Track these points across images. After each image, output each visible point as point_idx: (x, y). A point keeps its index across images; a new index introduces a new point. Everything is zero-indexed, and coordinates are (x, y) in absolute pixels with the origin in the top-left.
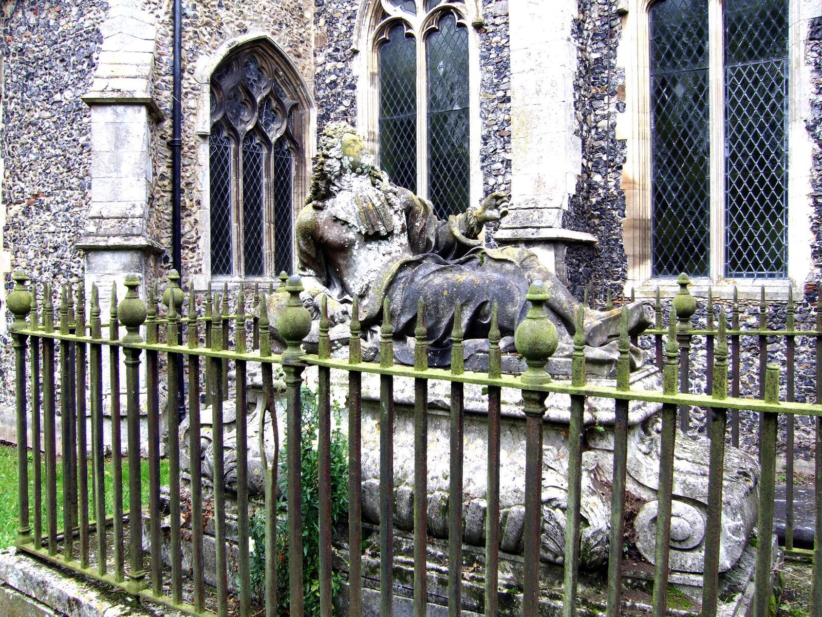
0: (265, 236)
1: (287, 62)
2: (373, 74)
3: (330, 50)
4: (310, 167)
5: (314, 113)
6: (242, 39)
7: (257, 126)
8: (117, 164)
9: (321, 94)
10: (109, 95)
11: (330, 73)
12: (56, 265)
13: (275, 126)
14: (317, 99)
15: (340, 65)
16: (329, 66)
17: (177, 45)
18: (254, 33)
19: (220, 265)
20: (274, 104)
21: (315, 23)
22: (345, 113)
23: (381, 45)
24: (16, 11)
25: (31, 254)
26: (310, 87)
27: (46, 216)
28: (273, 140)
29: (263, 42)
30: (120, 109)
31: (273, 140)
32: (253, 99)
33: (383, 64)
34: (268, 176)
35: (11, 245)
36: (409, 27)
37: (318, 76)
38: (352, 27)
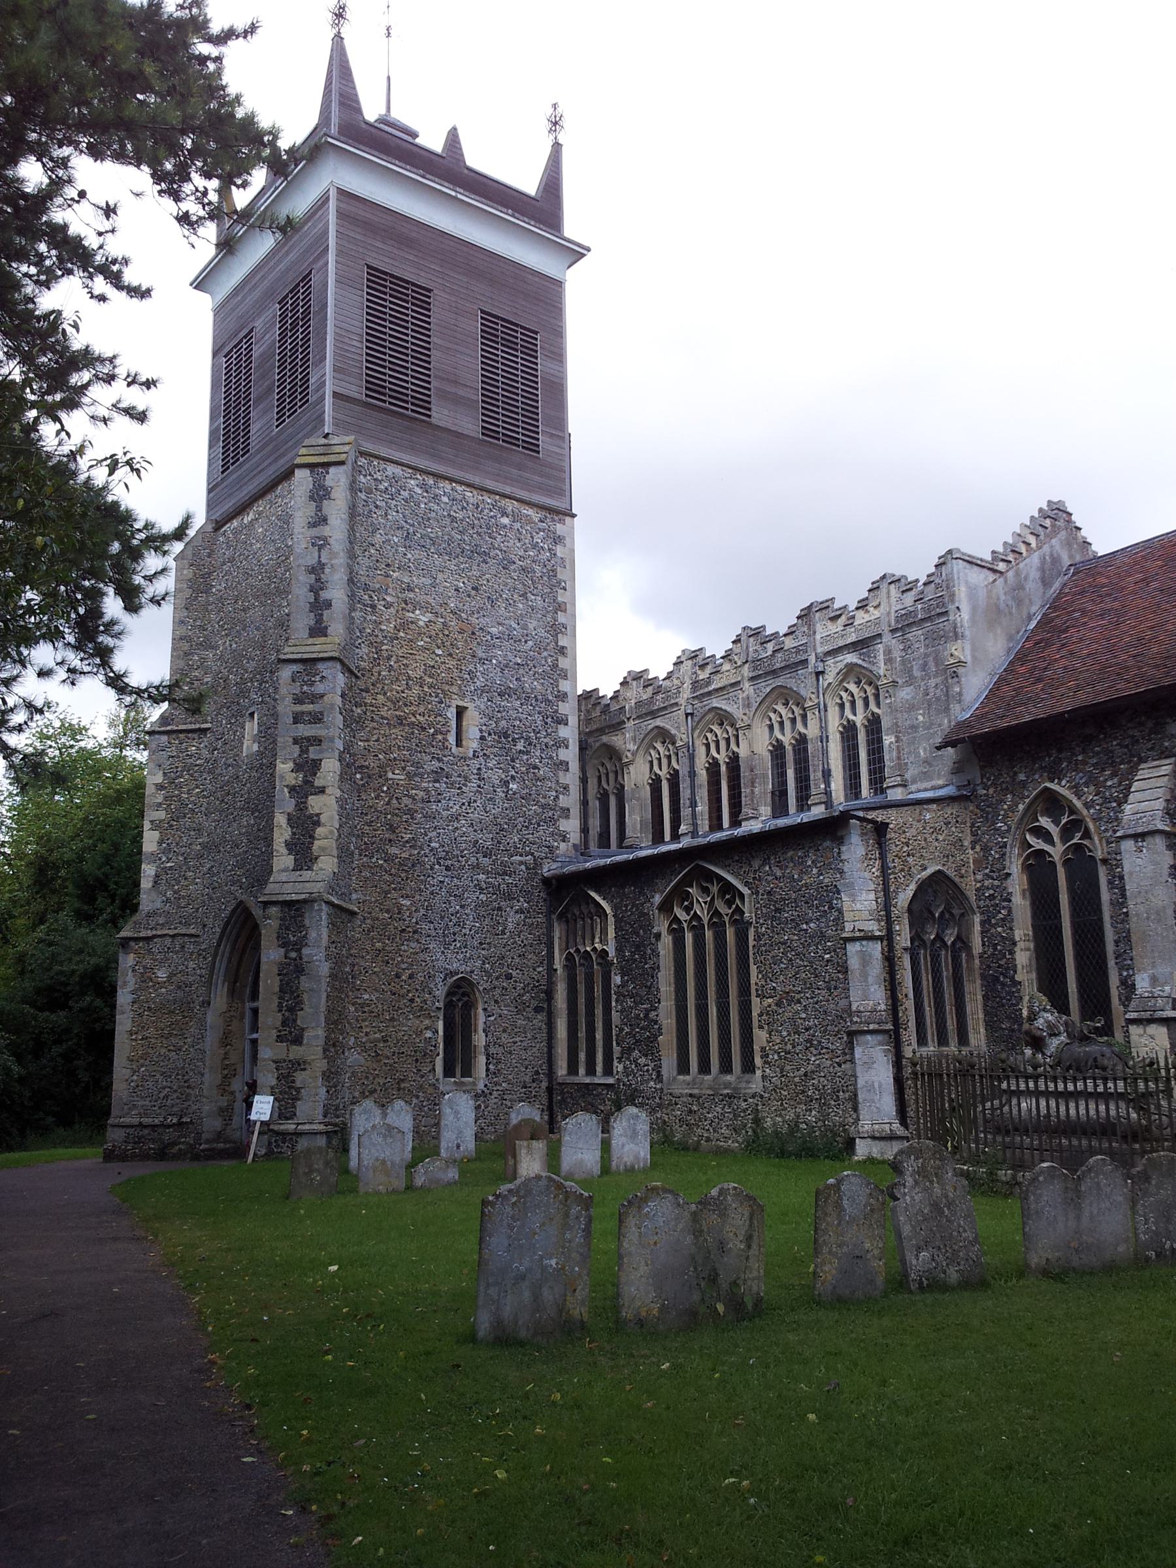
0: (948, 1017)
1: (955, 884)
2: (1024, 891)
3: (987, 871)
4: (977, 961)
5: (977, 919)
6: (925, 874)
7: (937, 935)
8: (864, 976)
9: (982, 903)
10: (858, 934)
11: (988, 889)
12: (809, 1041)
13: (948, 932)
14: (979, 907)
15: (996, 883)
16: (986, 883)
18: (929, 871)
19: (922, 1041)
20: (947, 916)
21: (973, 848)
22: (1003, 920)
23: (1027, 868)
24: (763, 865)
25: (785, 1033)
26: (972, 895)
27: (798, 1007)
28: (949, 943)
29: (939, 871)
30: (864, 943)
31: (949, 943)
33: (1031, 882)
34: (947, 970)
35: (766, 1027)
36: (1050, 856)
37: (977, 890)
38: (1004, 854)
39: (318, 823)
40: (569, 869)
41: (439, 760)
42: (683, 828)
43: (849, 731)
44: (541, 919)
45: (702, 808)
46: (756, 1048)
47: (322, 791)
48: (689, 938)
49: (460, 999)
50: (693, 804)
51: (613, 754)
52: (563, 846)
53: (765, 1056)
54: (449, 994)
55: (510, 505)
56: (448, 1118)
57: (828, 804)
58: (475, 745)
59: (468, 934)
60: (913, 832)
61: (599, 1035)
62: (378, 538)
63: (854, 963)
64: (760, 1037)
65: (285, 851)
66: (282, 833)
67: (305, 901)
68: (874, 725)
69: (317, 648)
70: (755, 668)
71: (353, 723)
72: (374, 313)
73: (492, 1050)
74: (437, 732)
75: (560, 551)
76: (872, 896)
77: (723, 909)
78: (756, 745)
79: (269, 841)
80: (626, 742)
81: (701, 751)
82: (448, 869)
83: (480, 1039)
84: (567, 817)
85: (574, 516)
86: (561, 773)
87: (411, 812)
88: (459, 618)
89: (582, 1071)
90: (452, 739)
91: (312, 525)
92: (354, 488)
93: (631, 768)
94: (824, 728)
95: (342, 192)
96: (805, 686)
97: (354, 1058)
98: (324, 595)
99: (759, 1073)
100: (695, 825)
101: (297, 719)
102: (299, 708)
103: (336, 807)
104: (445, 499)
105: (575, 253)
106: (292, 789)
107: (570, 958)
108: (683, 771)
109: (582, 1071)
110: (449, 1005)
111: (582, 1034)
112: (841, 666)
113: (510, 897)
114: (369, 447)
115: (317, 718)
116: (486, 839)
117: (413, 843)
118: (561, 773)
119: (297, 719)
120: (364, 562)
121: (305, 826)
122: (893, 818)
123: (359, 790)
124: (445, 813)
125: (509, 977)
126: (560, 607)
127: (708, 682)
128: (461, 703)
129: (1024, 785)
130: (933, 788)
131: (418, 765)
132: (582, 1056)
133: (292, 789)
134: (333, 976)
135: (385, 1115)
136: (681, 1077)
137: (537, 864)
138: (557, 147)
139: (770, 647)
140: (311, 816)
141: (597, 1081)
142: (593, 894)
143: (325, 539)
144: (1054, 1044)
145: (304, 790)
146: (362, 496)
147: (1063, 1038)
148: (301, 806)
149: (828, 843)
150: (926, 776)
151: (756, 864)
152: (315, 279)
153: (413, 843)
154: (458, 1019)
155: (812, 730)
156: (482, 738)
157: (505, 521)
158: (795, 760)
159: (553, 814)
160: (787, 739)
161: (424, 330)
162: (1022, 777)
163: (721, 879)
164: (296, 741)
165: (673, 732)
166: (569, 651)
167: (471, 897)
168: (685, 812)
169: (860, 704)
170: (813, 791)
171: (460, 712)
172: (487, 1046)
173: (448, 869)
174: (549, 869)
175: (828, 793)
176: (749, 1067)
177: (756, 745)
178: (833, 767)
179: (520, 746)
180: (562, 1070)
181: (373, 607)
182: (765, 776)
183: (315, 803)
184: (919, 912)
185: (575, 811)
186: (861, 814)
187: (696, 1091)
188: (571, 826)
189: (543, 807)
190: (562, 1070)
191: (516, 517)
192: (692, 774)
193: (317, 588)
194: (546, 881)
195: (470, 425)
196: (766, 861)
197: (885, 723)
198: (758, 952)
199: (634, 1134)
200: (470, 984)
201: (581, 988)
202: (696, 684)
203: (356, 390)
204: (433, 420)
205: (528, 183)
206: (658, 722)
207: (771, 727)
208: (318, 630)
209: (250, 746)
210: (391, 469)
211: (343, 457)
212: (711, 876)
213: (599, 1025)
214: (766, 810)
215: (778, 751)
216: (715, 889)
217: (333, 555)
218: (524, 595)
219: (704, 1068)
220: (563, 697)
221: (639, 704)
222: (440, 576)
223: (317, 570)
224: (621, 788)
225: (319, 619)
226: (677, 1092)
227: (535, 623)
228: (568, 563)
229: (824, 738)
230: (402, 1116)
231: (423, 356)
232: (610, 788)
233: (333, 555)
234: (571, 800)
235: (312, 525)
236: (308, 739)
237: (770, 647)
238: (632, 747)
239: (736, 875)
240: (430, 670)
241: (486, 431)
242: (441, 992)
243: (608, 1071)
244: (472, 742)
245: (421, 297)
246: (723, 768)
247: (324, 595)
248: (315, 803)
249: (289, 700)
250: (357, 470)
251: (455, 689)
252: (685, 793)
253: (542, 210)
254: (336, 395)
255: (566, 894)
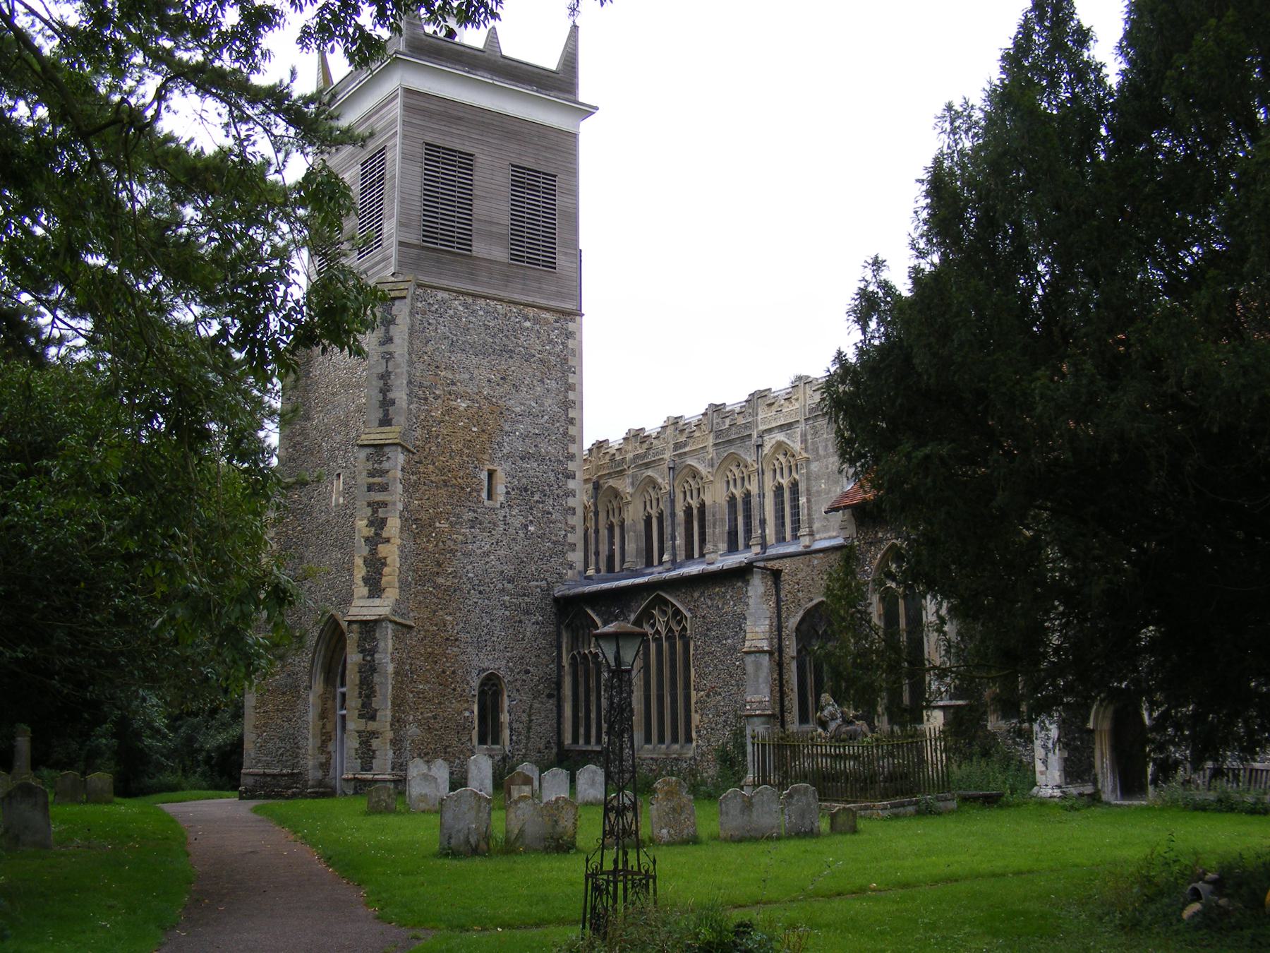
8: (757, 677)
17: (779, 616)
18: (815, 602)
23: (882, 599)
27: (719, 698)
32: (817, 632)
39: (385, 564)
40: (572, 592)
41: (474, 511)
42: (666, 557)
43: (779, 489)
44: (552, 628)
45: (680, 541)
46: (693, 726)
47: (388, 541)
48: (653, 646)
49: (491, 689)
50: (673, 538)
51: (616, 494)
52: (570, 572)
53: (698, 731)
54: (482, 684)
55: (531, 312)
56: (473, 772)
57: (764, 546)
58: (501, 498)
59: (495, 642)
60: (804, 574)
61: (593, 715)
62: (429, 348)
63: (750, 669)
64: (696, 718)
65: (361, 583)
66: (360, 571)
67: (376, 621)
68: (795, 485)
69: (383, 436)
70: (717, 437)
71: (409, 488)
72: (429, 179)
73: (515, 725)
74: (472, 490)
75: (570, 343)
76: (767, 622)
77: (676, 628)
78: (716, 496)
79: (350, 571)
80: (625, 486)
81: (680, 497)
82: (480, 592)
83: (505, 718)
84: (574, 550)
85: (582, 315)
86: (569, 517)
87: (453, 552)
88: (491, 403)
89: (581, 741)
90: (484, 495)
91: (382, 344)
92: (412, 313)
93: (631, 508)
94: (761, 487)
95: (408, 92)
96: (750, 458)
97: (413, 730)
98: (391, 395)
99: (694, 743)
100: (674, 555)
101: (370, 488)
102: (371, 480)
103: (397, 552)
104: (481, 313)
105: (587, 111)
106: (367, 539)
107: (574, 657)
108: (667, 513)
109: (581, 741)
110: (482, 693)
111: (582, 714)
112: (774, 441)
113: (528, 612)
114: (425, 279)
115: (384, 488)
116: (509, 570)
117: (455, 574)
118: (569, 517)
119: (370, 488)
120: (420, 366)
121: (375, 565)
122: (786, 566)
123: (415, 537)
124: (478, 552)
125: (527, 672)
126: (571, 387)
127: (685, 444)
128: (491, 467)
129: (881, 541)
130: (830, 538)
131: (459, 516)
132: (582, 730)
133: (367, 539)
134: (397, 673)
135: (430, 769)
136: (647, 746)
137: (550, 587)
138: (575, 28)
139: (727, 421)
140: (380, 560)
141: (589, 748)
142: (590, 612)
143: (391, 354)
144: (833, 726)
145: (375, 541)
146: (419, 317)
147: (839, 721)
148: (373, 552)
149: (740, 584)
150: (826, 528)
151: (696, 595)
152: (389, 156)
153: (455, 574)
154: (489, 703)
155: (754, 488)
156: (508, 493)
157: (528, 324)
158: (742, 507)
159: (562, 547)
160: (738, 493)
161: (468, 188)
162: (880, 535)
163: (673, 605)
164: (369, 505)
165: (660, 480)
166: (577, 421)
167: (499, 613)
168: (668, 544)
169: (786, 471)
170: (754, 535)
171: (491, 474)
172: (510, 724)
173: (480, 592)
174: (559, 591)
175: (763, 537)
176: (689, 740)
177: (716, 496)
178: (767, 517)
179: (536, 498)
180: (568, 740)
181: (426, 399)
182: (722, 520)
183: (383, 550)
184: (806, 630)
185: (580, 545)
186: (761, 564)
187: (655, 756)
188: (577, 557)
189: (555, 543)
190: (568, 740)
191: (536, 320)
192: (673, 515)
193: (385, 390)
194: (556, 600)
195: (500, 254)
196: (702, 594)
197: (802, 487)
198: (695, 659)
199: (593, 784)
200: (498, 677)
201: (582, 680)
202: (677, 446)
203: (414, 237)
204: (474, 254)
205: (550, 60)
206: (650, 473)
207: (728, 482)
208: (386, 421)
209: (337, 499)
210: (441, 295)
211: (404, 293)
212: (666, 602)
213: (593, 708)
214: (723, 546)
215: (732, 499)
216: (670, 612)
217: (397, 366)
218: (542, 381)
219: (661, 740)
220: (571, 457)
221: (636, 457)
222: (476, 372)
223: (385, 376)
224: (623, 522)
225: (386, 414)
226: (643, 757)
227: (550, 401)
228: (577, 353)
229: (762, 495)
230: (441, 771)
231: (467, 202)
232: (615, 521)
233: (397, 366)
234: (576, 538)
235: (382, 344)
236: (378, 503)
237: (727, 421)
238: (629, 490)
239: (682, 603)
240: (469, 443)
241: (514, 257)
242: (475, 683)
243: (599, 741)
244: (500, 497)
245: (466, 161)
246: (695, 512)
247: (391, 395)
248: (383, 550)
249: (365, 473)
250: (416, 298)
251: (486, 457)
252: (667, 530)
253: (559, 83)
254: (401, 244)
255: (571, 612)
